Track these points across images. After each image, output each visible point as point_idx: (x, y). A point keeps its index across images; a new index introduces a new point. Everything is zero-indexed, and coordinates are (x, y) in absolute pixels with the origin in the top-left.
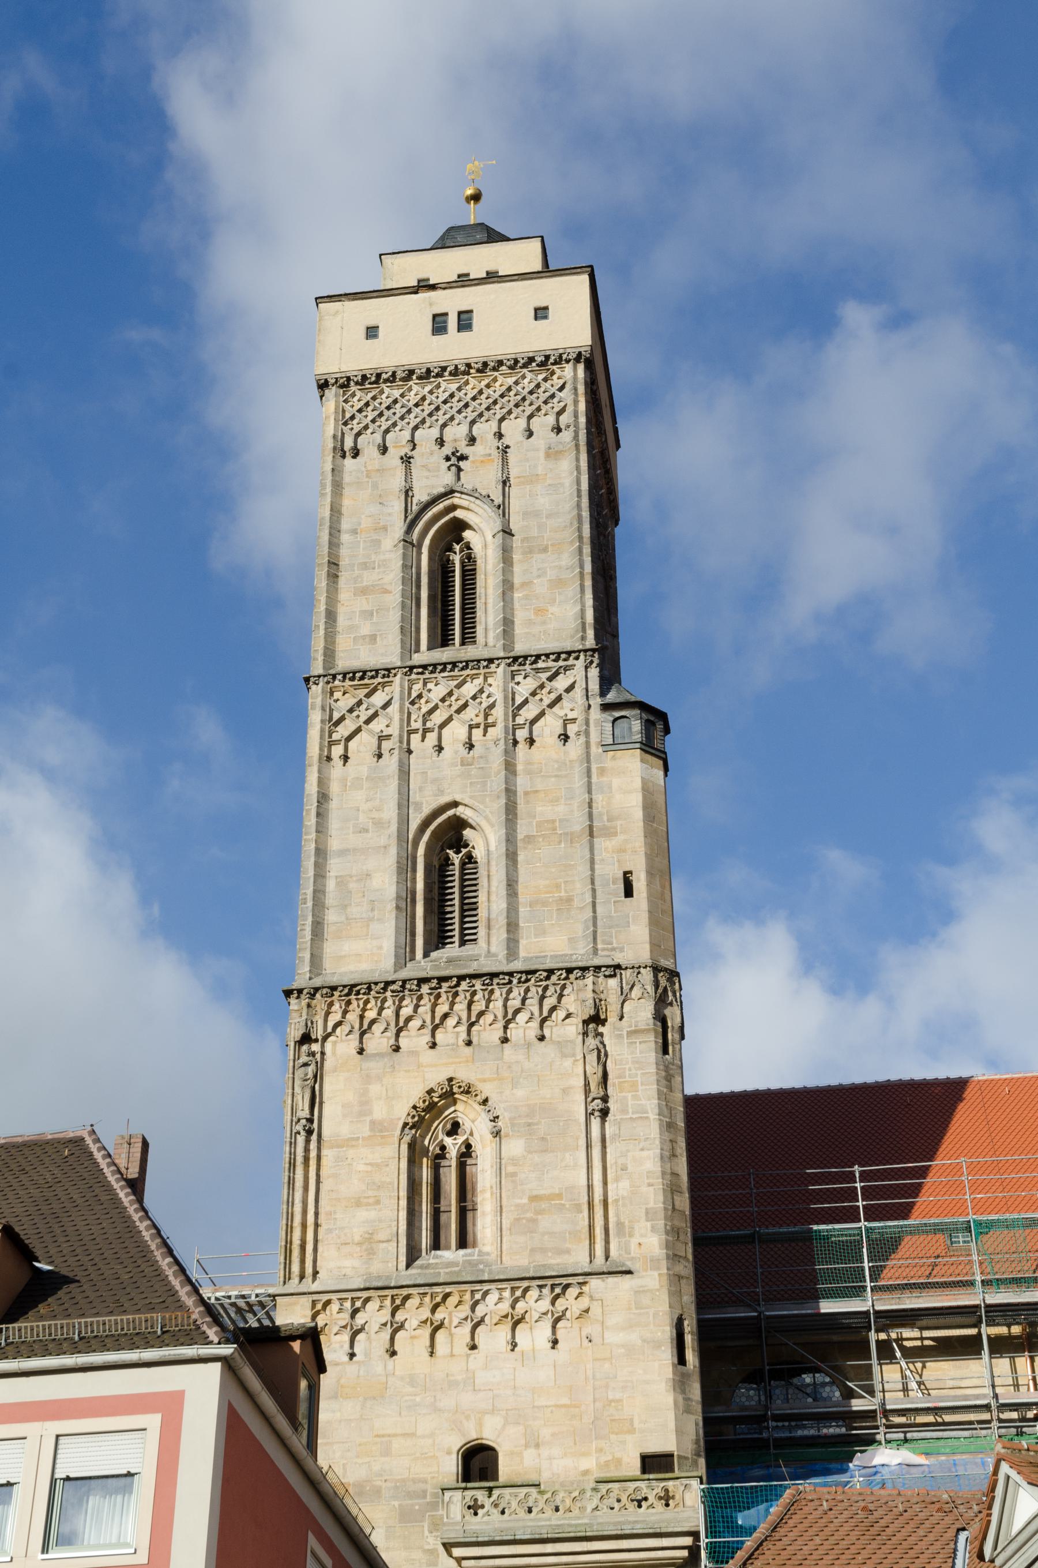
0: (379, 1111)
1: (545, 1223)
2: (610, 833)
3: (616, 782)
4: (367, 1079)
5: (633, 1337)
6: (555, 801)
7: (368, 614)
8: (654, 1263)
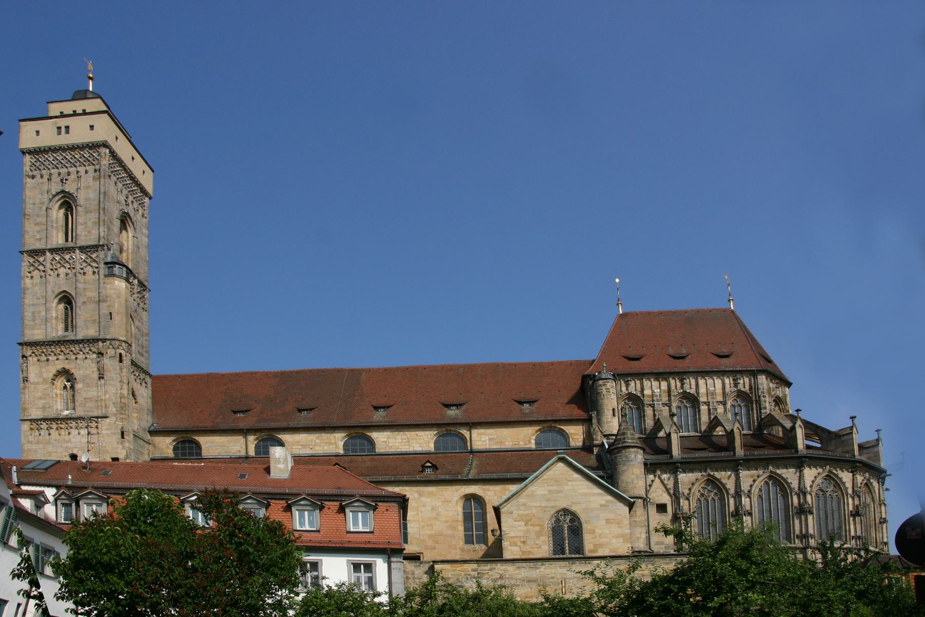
1: (88, 405)
2: (105, 301)
5: (109, 432)
7: (38, 232)
8: (115, 415)
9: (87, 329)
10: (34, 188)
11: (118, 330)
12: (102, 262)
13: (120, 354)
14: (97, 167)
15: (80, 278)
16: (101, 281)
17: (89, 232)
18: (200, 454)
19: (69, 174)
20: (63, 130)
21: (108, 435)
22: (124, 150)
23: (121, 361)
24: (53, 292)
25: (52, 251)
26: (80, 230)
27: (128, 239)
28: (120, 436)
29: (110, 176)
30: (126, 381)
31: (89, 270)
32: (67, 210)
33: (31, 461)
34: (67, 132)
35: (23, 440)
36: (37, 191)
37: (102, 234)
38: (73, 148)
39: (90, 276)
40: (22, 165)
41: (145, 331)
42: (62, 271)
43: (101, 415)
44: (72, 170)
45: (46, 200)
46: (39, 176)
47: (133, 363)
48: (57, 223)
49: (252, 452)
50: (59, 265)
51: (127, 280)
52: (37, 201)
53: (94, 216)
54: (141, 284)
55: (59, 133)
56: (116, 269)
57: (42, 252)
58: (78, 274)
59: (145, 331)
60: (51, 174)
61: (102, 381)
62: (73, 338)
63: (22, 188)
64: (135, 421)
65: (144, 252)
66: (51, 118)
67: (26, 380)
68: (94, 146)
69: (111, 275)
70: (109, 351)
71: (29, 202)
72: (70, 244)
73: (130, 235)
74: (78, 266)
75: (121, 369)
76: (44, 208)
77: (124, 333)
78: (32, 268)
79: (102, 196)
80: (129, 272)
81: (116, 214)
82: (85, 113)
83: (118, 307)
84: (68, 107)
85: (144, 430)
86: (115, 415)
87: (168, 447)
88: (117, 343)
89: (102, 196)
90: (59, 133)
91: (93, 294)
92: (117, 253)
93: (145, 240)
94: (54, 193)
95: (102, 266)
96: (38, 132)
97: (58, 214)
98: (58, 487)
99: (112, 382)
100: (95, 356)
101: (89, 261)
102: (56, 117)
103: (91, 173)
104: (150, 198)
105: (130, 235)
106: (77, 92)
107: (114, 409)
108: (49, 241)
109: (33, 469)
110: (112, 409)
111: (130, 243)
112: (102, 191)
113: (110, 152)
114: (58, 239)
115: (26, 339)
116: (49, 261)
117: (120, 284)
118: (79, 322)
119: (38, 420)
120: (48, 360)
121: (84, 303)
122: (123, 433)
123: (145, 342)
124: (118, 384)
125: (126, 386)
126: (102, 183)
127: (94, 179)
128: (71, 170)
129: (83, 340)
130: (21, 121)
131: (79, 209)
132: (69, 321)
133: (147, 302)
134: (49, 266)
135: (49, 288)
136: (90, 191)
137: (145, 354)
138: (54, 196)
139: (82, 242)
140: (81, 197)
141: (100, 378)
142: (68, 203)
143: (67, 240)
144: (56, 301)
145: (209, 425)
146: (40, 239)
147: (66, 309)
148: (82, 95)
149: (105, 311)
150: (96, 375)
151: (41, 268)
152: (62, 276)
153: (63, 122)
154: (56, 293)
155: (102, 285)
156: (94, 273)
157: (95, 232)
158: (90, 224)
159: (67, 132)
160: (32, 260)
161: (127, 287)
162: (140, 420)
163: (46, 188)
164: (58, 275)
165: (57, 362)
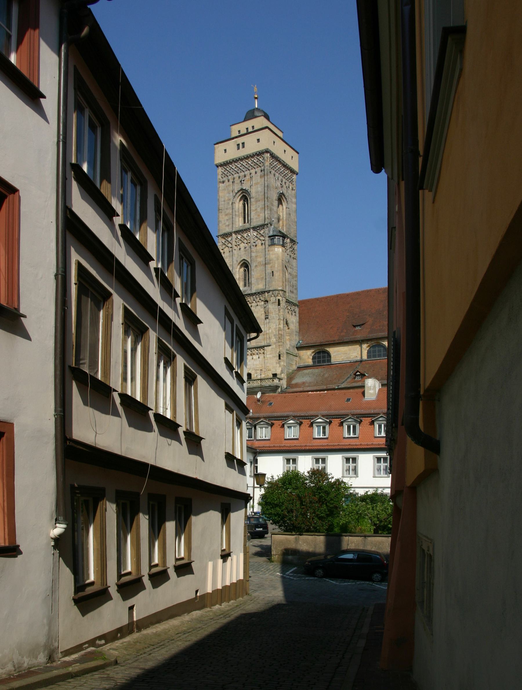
2: (269, 263)
3: (271, 253)
5: (271, 356)
6: (261, 258)
7: (227, 220)
8: (275, 343)
9: (258, 284)
10: (224, 190)
11: (277, 284)
12: (267, 236)
13: (279, 300)
14: (263, 168)
15: (254, 249)
16: (267, 250)
17: (259, 215)
18: (329, 361)
19: (245, 176)
20: (241, 146)
21: (270, 358)
23: (279, 304)
24: (237, 261)
25: (237, 232)
26: (253, 215)
28: (278, 358)
29: (270, 172)
30: (282, 318)
31: (259, 243)
32: (244, 201)
36: (226, 192)
37: (266, 216)
38: (247, 157)
39: (259, 247)
41: (294, 274)
42: (242, 246)
43: (266, 344)
44: (247, 173)
45: (232, 197)
46: (227, 181)
48: (238, 212)
49: (365, 357)
50: (240, 242)
51: (283, 246)
52: (226, 198)
53: (261, 204)
55: (238, 148)
56: (276, 240)
57: (229, 235)
58: (252, 247)
59: (294, 274)
60: (234, 178)
61: (267, 320)
62: (249, 292)
63: (218, 192)
66: (233, 138)
68: (260, 154)
69: (273, 244)
70: (272, 298)
71: (221, 199)
72: (247, 225)
74: (252, 241)
75: (279, 310)
76: (231, 203)
77: (281, 284)
78: (224, 246)
79: (266, 189)
83: (277, 266)
84: (242, 127)
86: (275, 343)
88: (277, 292)
89: (266, 189)
90: (238, 148)
91: (261, 259)
94: (236, 192)
95: (267, 239)
96: (225, 150)
97: (239, 205)
99: (273, 321)
100: (263, 303)
101: (258, 236)
102: (236, 137)
103: (259, 173)
107: (275, 340)
108: (234, 226)
110: (274, 340)
112: (266, 185)
113: (270, 155)
114: (239, 223)
116: (234, 240)
117: (278, 250)
118: (253, 280)
121: (256, 266)
122: (280, 355)
123: (294, 282)
124: (277, 321)
125: (282, 322)
126: (266, 179)
127: (261, 177)
128: (246, 173)
129: (255, 293)
130: (215, 144)
131: (252, 200)
133: (296, 252)
135: (235, 258)
136: (259, 186)
137: (295, 291)
138: (236, 194)
139: (254, 223)
141: (266, 318)
142: (245, 196)
143: (245, 222)
144: (239, 267)
146: (229, 225)
147: (245, 271)
148: (251, 115)
149: (269, 271)
151: (230, 245)
152: (242, 249)
153: (240, 140)
154: (239, 261)
155: (267, 252)
156: (262, 244)
157: (262, 215)
158: (259, 210)
159: (243, 147)
160: (223, 241)
161: (283, 251)
163: (231, 188)
164: (240, 249)
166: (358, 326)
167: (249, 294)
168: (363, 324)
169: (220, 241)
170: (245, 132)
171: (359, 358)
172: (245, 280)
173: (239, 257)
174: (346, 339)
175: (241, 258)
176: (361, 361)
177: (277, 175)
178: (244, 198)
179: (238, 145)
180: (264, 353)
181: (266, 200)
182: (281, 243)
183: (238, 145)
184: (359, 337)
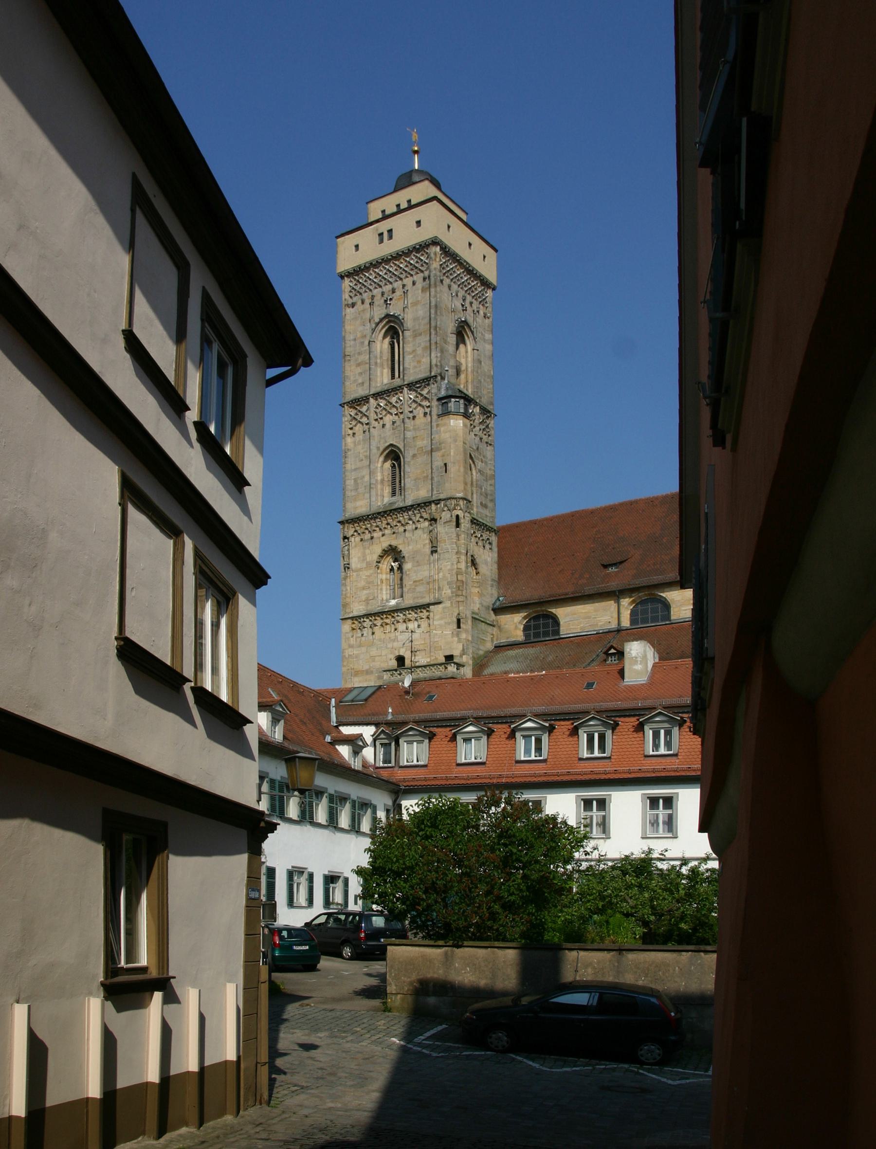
0: (369, 558)
1: (418, 589)
2: (438, 449)
3: (442, 429)
4: (364, 548)
5: (442, 622)
6: (423, 439)
7: (360, 374)
8: (450, 598)
9: (418, 490)
10: (355, 319)
11: (454, 486)
12: (435, 398)
13: (457, 516)
14: (426, 273)
15: (409, 424)
16: (434, 424)
17: (419, 362)
18: (557, 632)
19: (393, 291)
21: (441, 626)
22: (459, 239)
23: (458, 525)
24: (378, 448)
25: (377, 395)
26: (409, 361)
27: (466, 355)
28: (455, 626)
29: (442, 281)
30: (464, 551)
31: (420, 411)
32: (392, 338)
33: (351, 690)
34: (390, 237)
35: (344, 645)
36: (358, 322)
37: (434, 362)
39: (421, 420)
40: (340, 292)
42: (388, 419)
43: (433, 601)
44: (398, 285)
45: (369, 332)
46: (359, 302)
47: (474, 521)
48: (381, 357)
50: (384, 413)
51: (466, 415)
52: (359, 335)
53: (423, 340)
54: (484, 411)
55: (381, 241)
56: (452, 405)
57: (365, 400)
58: (407, 420)
60: (373, 297)
61: (436, 555)
62: (401, 505)
63: (341, 322)
64: (476, 599)
65: (487, 366)
66: (371, 224)
67: (347, 567)
68: (421, 248)
69: (446, 413)
70: (444, 513)
71: (349, 337)
72: (397, 382)
73: (469, 348)
74: (407, 409)
75: (458, 536)
76: (367, 343)
77: (461, 487)
78: (354, 423)
79: (433, 311)
80: (468, 400)
81: (450, 327)
82: (411, 207)
83: (454, 454)
84: (389, 204)
85: (487, 608)
86: (450, 598)
87: (516, 628)
88: (453, 502)
89: (433, 311)
90: (381, 241)
91: (424, 443)
92: (453, 380)
93: (489, 347)
94: (377, 320)
95: (435, 403)
96: (357, 247)
97: (382, 345)
98: (377, 725)
99: (447, 556)
100: (427, 524)
101: (418, 400)
102: (377, 221)
103: (420, 284)
104: (494, 289)
105: (469, 348)
106: (400, 178)
107: (449, 591)
108: (373, 384)
109: (352, 701)
110: (447, 592)
111: (470, 359)
112: (433, 304)
113: (442, 248)
114: (383, 379)
115: (348, 515)
116: (372, 409)
117: (457, 423)
118: (408, 482)
119: (360, 617)
120: (372, 538)
121: (414, 456)
122: (459, 621)
124: (455, 557)
125: (463, 558)
126: (433, 293)
127: (423, 290)
128: (396, 285)
129: (412, 506)
130: (337, 237)
131: (407, 333)
132: (396, 485)
134: (373, 416)
135: (374, 444)
136: (419, 307)
138: (377, 324)
139: (410, 378)
140: (409, 323)
141: (433, 552)
142: (393, 328)
143: (393, 377)
144: (382, 459)
145: (570, 590)
146: (363, 383)
147: (393, 466)
148: (406, 181)
149: (438, 463)
150: (428, 550)
151: (364, 420)
152: (388, 425)
154: (381, 449)
155: (434, 429)
156: (425, 414)
157: (425, 360)
158: (419, 351)
159: (390, 237)
160: (353, 412)
161: (465, 425)
162: (482, 595)
163: (367, 316)
164: (384, 426)
165: (382, 539)
166: (611, 565)
167: (401, 508)
168: (621, 563)
169: (346, 412)
170: (395, 209)
171: (614, 625)
172: (393, 483)
173: (382, 441)
174: (588, 590)
175: (386, 442)
176: (619, 631)
177: (455, 287)
178: (391, 333)
179: (381, 235)
180: (428, 618)
181: (433, 332)
182: (462, 410)
183: (381, 235)
184: (614, 585)
